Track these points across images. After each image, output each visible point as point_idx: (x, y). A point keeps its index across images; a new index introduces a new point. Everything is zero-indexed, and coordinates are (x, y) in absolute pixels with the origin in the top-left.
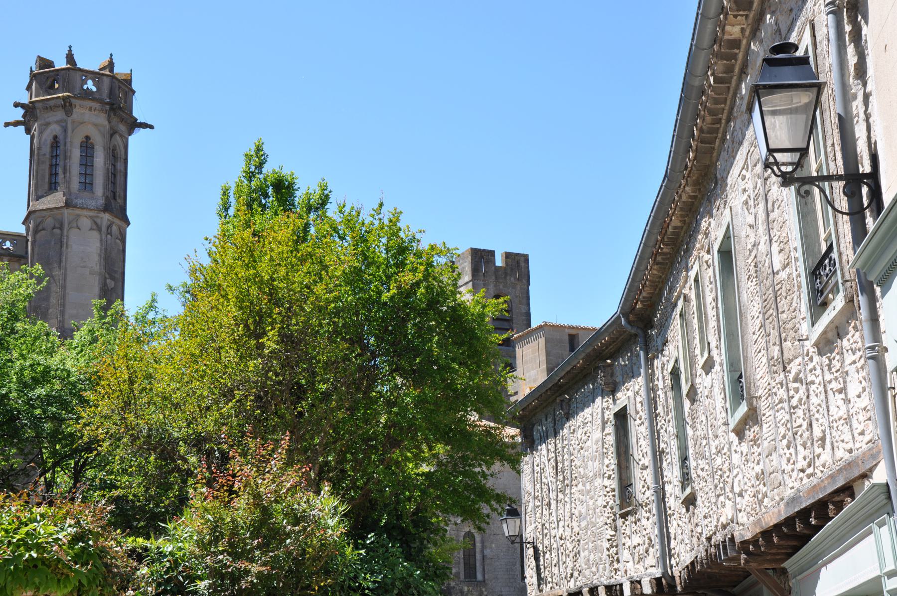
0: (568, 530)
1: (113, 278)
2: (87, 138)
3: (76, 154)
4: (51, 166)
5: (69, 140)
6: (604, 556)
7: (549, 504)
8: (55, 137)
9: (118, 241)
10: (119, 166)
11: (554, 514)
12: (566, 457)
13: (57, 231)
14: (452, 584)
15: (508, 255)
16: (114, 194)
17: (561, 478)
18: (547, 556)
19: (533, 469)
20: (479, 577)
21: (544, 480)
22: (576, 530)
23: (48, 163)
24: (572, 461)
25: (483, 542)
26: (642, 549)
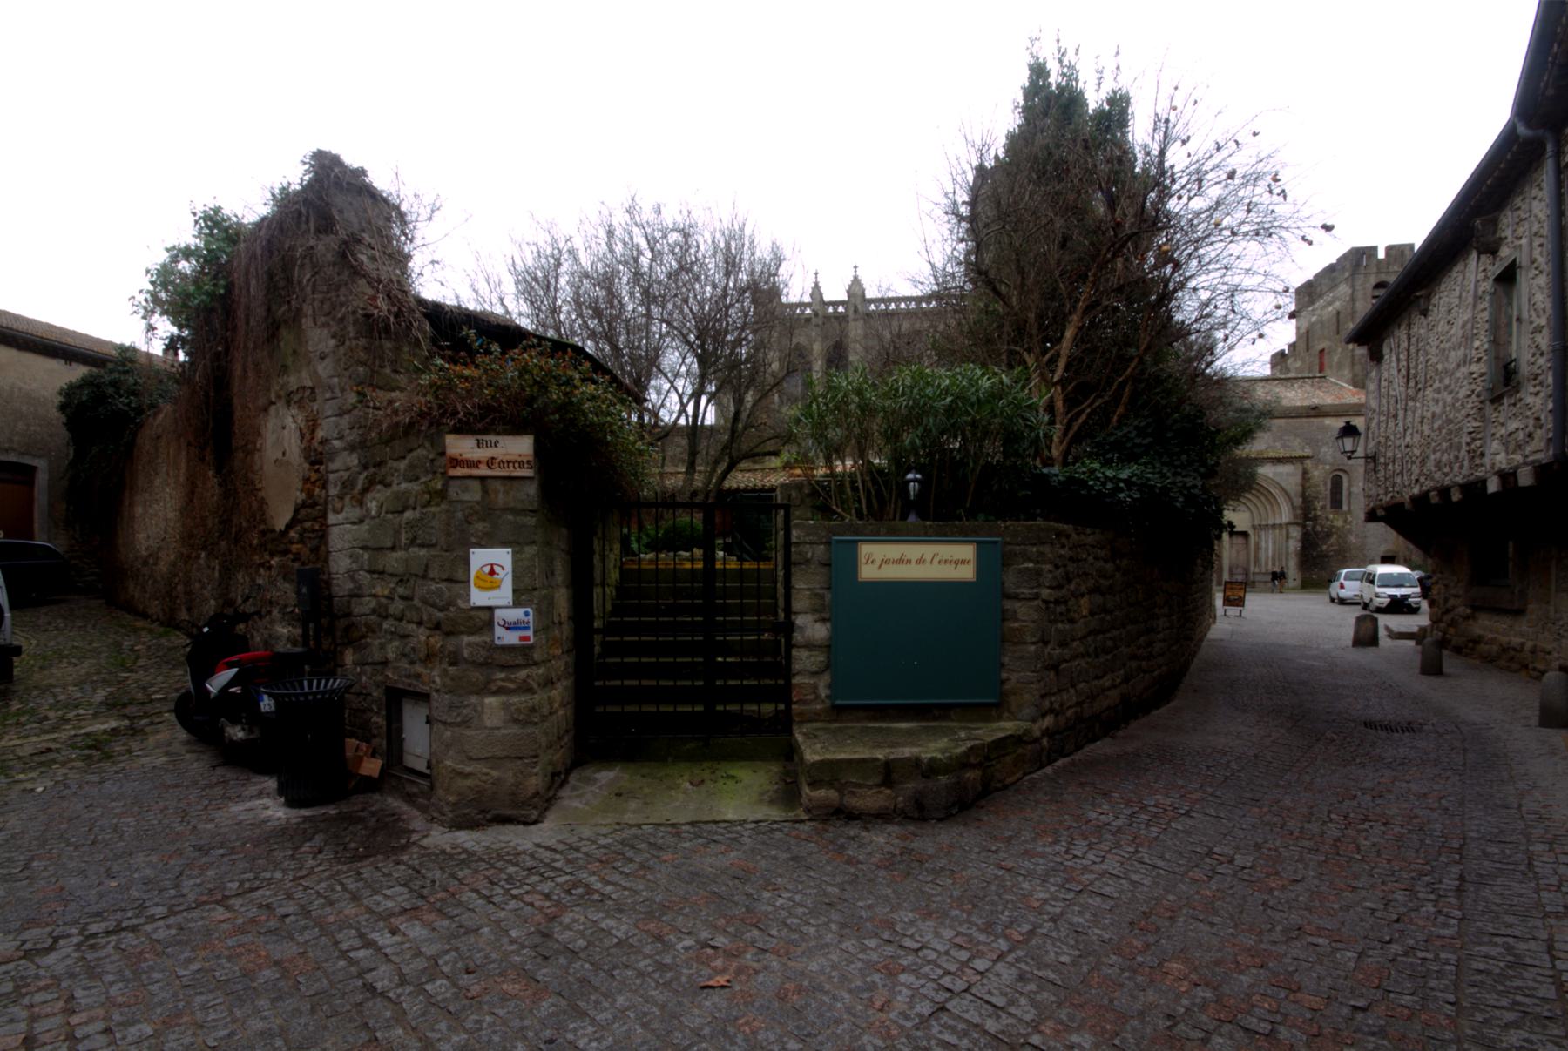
0: (1417, 437)
6: (1463, 453)
7: (1395, 417)
11: (1401, 425)
12: (1421, 359)
14: (1319, 513)
15: (1389, 249)
17: (1412, 384)
18: (1390, 467)
19: (1379, 386)
20: (1345, 508)
21: (1392, 393)
22: (1427, 432)
24: (1427, 361)
25: (1350, 481)
26: (1521, 435)
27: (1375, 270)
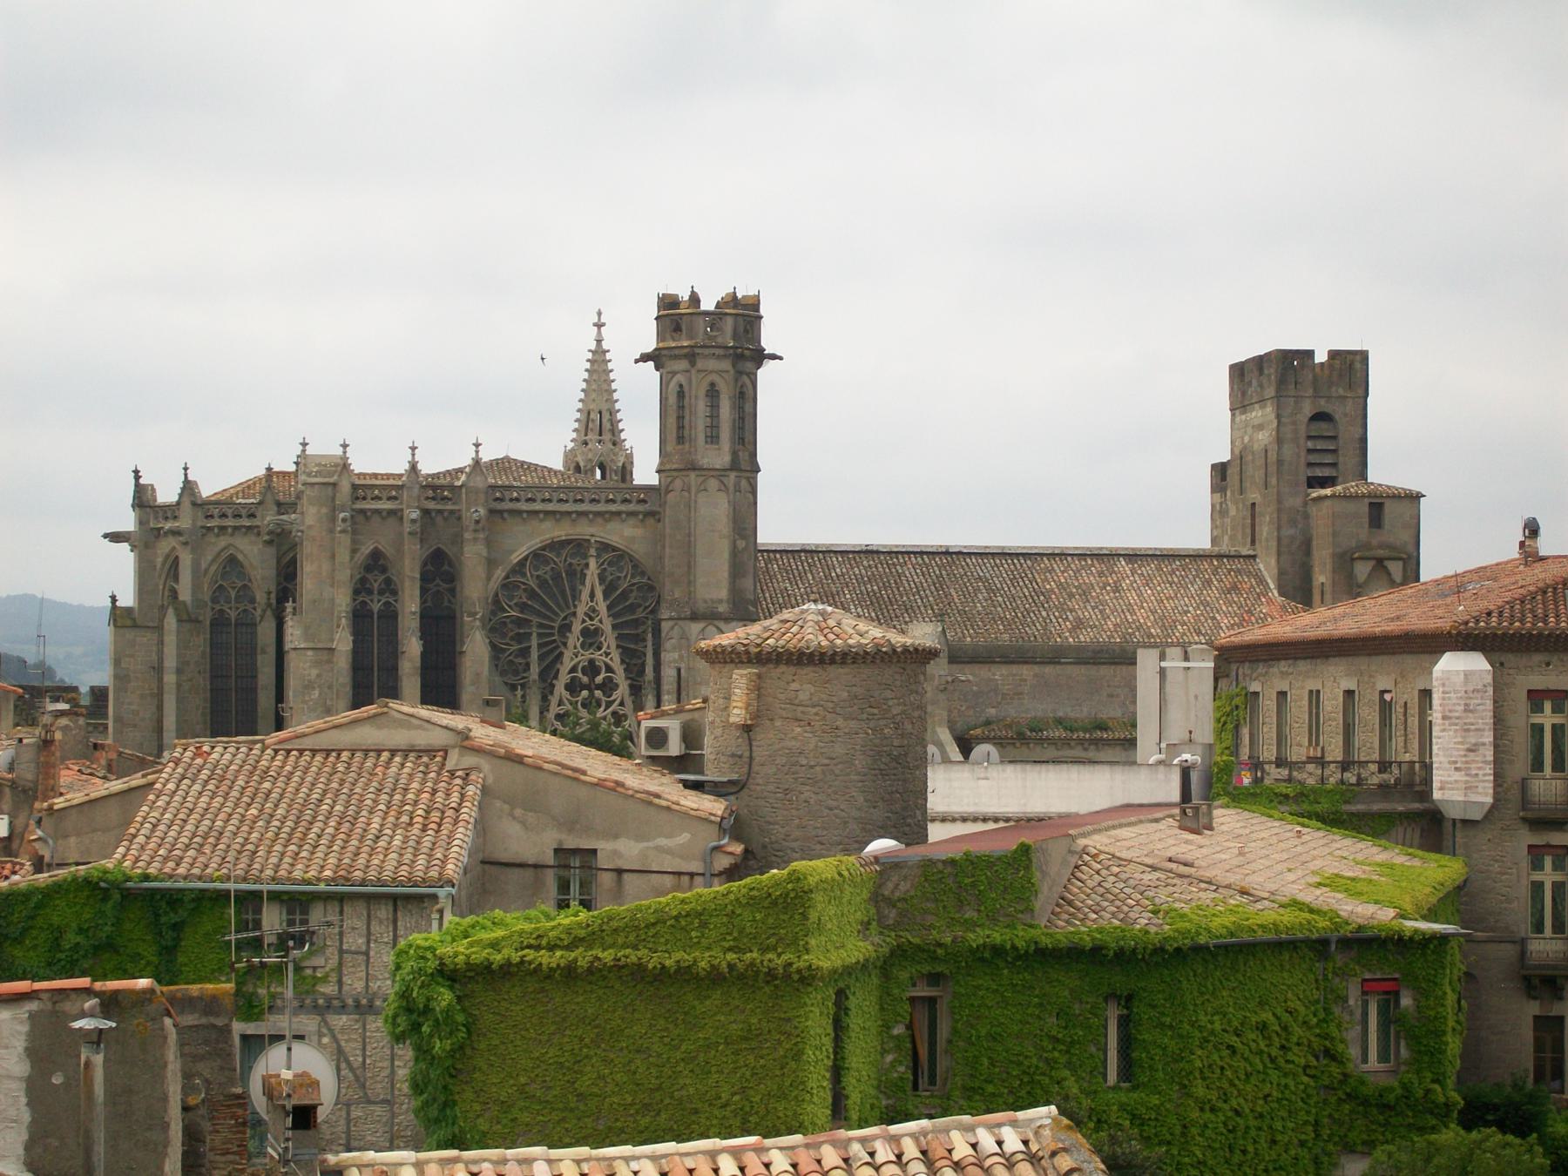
1: (743, 537)
2: (713, 385)
3: (702, 407)
4: (678, 418)
5: (693, 392)
8: (681, 386)
9: (750, 496)
10: (748, 408)
13: (686, 494)
16: (742, 440)
23: (675, 416)
27: (1310, 392)
